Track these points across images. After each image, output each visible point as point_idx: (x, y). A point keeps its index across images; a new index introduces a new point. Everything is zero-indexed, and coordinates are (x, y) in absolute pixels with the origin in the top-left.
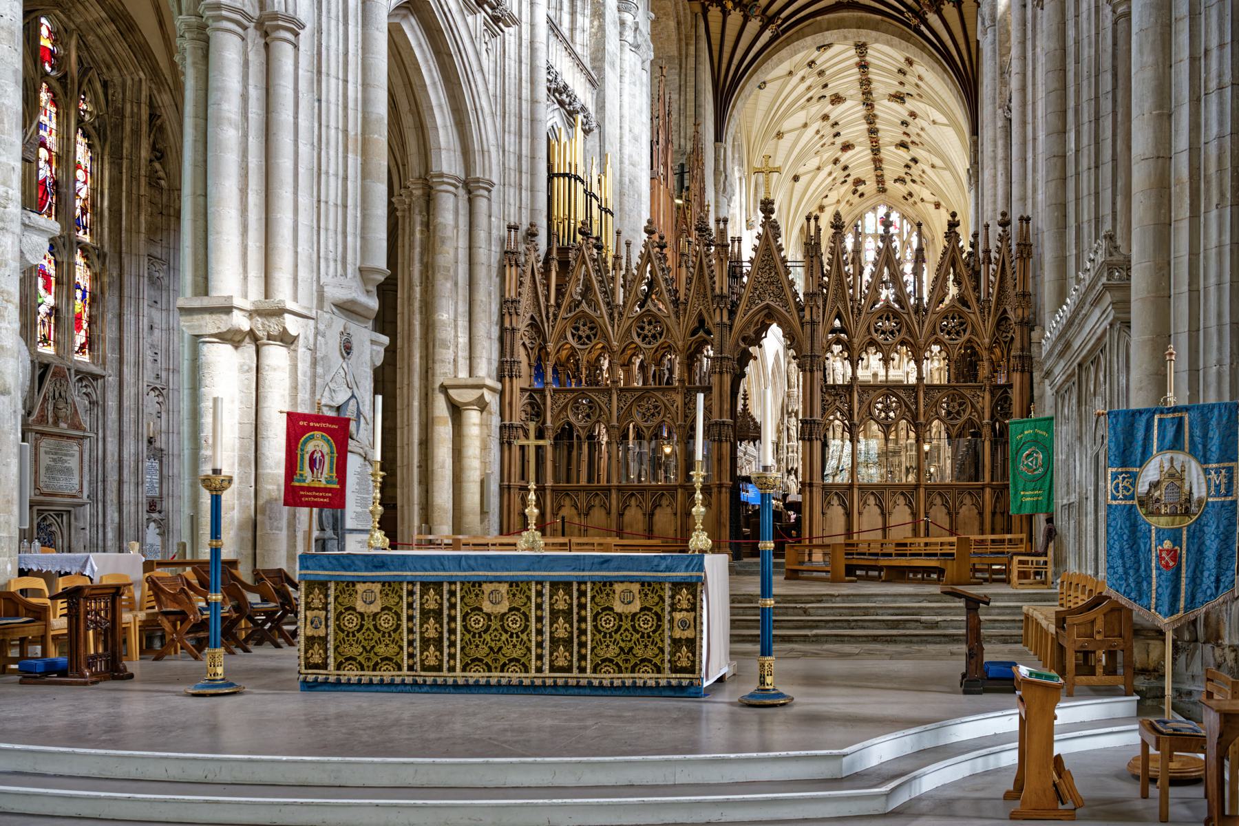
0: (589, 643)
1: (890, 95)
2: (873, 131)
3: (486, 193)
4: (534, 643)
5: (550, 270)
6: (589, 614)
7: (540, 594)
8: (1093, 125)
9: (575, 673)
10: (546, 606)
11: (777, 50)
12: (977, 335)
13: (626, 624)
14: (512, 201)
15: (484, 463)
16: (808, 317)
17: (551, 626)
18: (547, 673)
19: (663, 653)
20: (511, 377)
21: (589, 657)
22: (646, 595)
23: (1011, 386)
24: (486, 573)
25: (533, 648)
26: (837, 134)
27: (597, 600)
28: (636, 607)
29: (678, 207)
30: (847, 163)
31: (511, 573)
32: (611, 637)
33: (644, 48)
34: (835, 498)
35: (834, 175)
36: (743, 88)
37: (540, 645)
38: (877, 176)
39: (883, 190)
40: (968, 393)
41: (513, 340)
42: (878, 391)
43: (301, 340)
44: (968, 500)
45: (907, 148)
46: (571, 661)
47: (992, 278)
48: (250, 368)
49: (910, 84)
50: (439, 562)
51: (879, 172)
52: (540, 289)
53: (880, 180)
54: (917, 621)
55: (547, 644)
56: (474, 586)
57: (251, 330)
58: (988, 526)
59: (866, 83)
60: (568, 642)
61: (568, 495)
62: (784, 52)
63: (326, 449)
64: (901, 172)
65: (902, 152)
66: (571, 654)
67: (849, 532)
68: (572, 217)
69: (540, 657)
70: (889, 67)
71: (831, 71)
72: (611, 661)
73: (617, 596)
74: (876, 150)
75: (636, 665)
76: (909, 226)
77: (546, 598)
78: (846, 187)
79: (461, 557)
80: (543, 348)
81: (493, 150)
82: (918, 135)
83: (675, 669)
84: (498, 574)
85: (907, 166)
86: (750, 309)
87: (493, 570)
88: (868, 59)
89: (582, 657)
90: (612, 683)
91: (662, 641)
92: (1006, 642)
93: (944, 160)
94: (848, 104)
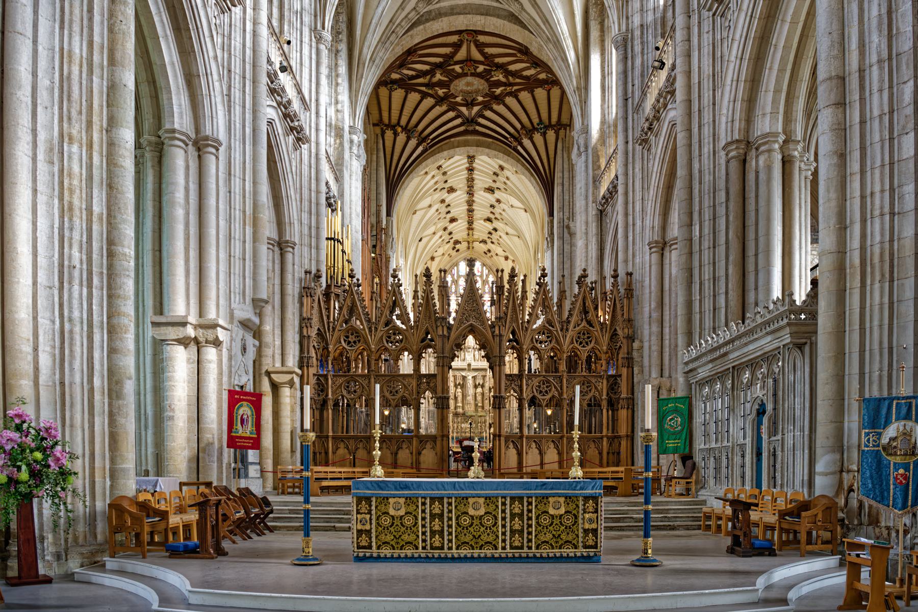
1: (486, 188)
2: (470, 211)
3: (291, 250)
4: (500, 533)
5: (330, 299)
6: (534, 515)
7: (504, 504)
8: (712, 222)
9: (526, 550)
10: (508, 511)
11: (425, 159)
12: (598, 344)
13: (557, 521)
15: (293, 421)
16: (497, 332)
17: (511, 522)
18: (508, 550)
19: (578, 537)
20: (308, 367)
21: (533, 540)
22: (568, 504)
24: (471, 492)
25: (500, 536)
26: (449, 212)
27: (539, 507)
28: (562, 511)
29: (374, 258)
31: (487, 492)
32: (547, 528)
33: (362, 157)
35: (443, 238)
36: (404, 182)
37: (504, 534)
40: (593, 380)
41: (309, 343)
42: (538, 378)
43: (224, 344)
44: (592, 445)
46: (523, 543)
47: (607, 309)
48: (194, 361)
49: (500, 182)
50: (526, 486)
52: (324, 311)
54: (631, 518)
55: (508, 533)
56: (463, 499)
57: (195, 337)
58: (605, 461)
59: (470, 181)
61: (342, 441)
62: (429, 161)
63: (249, 413)
64: (485, 236)
65: (488, 224)
66: (523, 539)
69: (504, 541)
71: (451, 172)
72: (547, 542)
73: (551, 505)
74: (470, 223)
75: (562, 544)
77: (508, 507)
78: (449, 245)
79: (455, 482)
80: (326, 348)
81: (296, 222)
82: (500, 214)
83: (585, 547)
84: (479, 492)
85: (490, 233)
87: (475, 490)
88: (474, 165)
89: (530, 541)
90: (548, 555)
91: (578, 530)
92: (688, 529)
93: (516, 230)
94: (458, 193)
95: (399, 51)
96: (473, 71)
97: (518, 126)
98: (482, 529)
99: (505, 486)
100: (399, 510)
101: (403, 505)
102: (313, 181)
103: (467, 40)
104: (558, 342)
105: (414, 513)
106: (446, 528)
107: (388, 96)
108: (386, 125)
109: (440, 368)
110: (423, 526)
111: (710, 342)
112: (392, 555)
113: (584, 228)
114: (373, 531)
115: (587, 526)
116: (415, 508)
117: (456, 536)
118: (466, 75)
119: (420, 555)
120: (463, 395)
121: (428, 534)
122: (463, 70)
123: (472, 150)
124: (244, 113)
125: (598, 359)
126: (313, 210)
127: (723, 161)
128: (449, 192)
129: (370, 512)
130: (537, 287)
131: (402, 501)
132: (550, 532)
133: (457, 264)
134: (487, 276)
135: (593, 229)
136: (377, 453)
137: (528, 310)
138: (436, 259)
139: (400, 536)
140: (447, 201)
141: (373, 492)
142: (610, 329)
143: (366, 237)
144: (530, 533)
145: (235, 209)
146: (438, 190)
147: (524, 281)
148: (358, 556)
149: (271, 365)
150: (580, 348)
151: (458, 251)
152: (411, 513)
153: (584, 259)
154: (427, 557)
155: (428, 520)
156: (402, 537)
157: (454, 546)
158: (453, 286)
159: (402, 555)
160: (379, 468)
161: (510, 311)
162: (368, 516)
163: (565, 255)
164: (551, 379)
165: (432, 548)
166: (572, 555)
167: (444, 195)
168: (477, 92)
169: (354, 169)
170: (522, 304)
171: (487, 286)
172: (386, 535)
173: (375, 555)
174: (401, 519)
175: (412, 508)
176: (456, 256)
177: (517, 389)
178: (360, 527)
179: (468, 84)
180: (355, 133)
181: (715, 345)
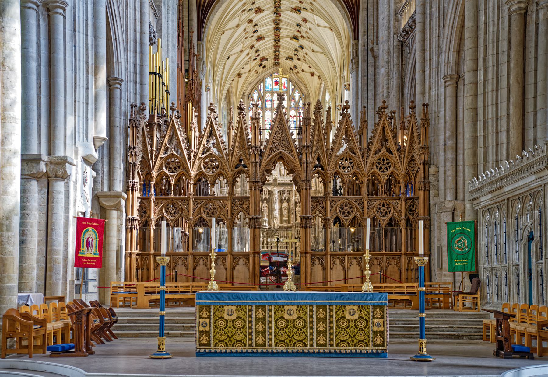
0: (334, 333)
1: (292, 8)
2: (277, 29)
4: (309, 333)
5: (153, 130)
6: (334, 320)
7: (311, 311)
9: (328, 347)
10: (314, 316)
12: (397, 169)
16: (304, 159)
17: (317, 325)
18: (315, 347)
19: (369, 337)
21: (334, 339)
22: (361, 311)
23: (417, 198)
24: (287, 301)
25: (309, 336)
26: (256, 31)
27: (338, 313)
28: (356, 316)
29: (187, 83)
30: (258, 48)
31: (299, 301)
34: (317, 260)
35: (250, 55)
37: (312, 334)
38: (275, 55)
39: (277, 64)
42: (341, 200)
45: (298, 40)
46: (326, 341)
48: (45, 192)
49: (307, 3)
50: (329, 297)
51: (277, 53)
53: (277, 58)
55: (315, 334)
60: (325, 333)
63: (94, 237)
64: (292, 54)
66: (326, 338)
67: (325, 278)
69: (312, 340)
72: (345, 341)
73: (347, 311)
76: (293, 87)
77: (314, 313)
78: (255, 61)
82: (307, 32)
84: (292, 301)
86: (271, 154)
87: (289, 300)
89: (331, 340)
90: (346, 351)
93: (322, 48)
94: (266, 13)
98: (295, 330)
99: (313, 297)
100: (231, 315)
101: (235, 312)
104: (358, 167)
105: (243, 318)
106: (267, 329)
109: (253, 191)
110: (250, 328)
111: (490, 176)
112: (226, 351)
113: (386, 57)
114: (212, 332)
115: (376, 329)
116: (244, 313)
117: (275, 336)
119: (247, 351)
120: (269, 209)
121: (254, 334)
125: (397, 182)
126: (137, 49)
127: (506, 14)
128: (256, 12)
129: (209, 317)
130: (341, 117)
131: (234, 308)
132: (347, 333)
133: (263, 80)
135: (395, 59)
136: (213, 271)
137: (332, 138)
138: (242, 76)
139: (232, 335)
140: (254, 20)
141: (212, 301)
142: (408, 155)
143: (180, 65)
144: (331, 334)
145: (79, 60)
146: (246, 11)
147: (328, 112)
148: (199, 352)
149: (100, 190)
150: (379, 172)
151: (264, 67)
152: (241, 318)
153: (385, 87)
154: (253, 352)
155: (253, 323)
156: (234, 337)
157: (273, 344)
159: (234, 351)
160: (214, 283)
161: (315, 140)
162: (208, 320)
163: (369, 77)
164: (353, 201)
165: (256, 345)
166: (364, 351)
167: (252, 15)
170: (327, 133)
171: (293, 102)
172: (221, 335)
173: (213, 351)
174: (233, 323)
175: (241, 314)
176: (262, 73)
177: (322, 210)
178: (201, 329)
181: (493, 179)
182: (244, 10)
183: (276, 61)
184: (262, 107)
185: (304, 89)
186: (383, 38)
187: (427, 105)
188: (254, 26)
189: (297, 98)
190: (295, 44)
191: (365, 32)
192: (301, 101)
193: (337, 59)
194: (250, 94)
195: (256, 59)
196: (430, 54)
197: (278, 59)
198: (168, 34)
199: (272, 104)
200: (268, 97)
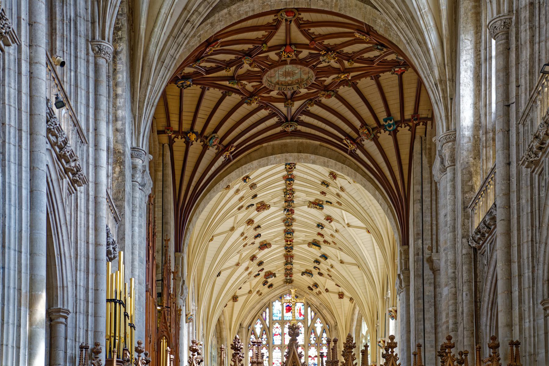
1: (310, 202)
2: (289, 232)
14: (81, 326)
26: (259, 236)
30: (262, 259)
38: (286, 269)
39: (289, 281)
45: (319, 246)
49: (332, 194)
51: (289, 266)
53: (289, 273)
64: (310, 266)
68: (117, 335)
70: (313, 179)
74: (289, 248)
76: (313, 314)
78: (258, 278)
82: (332, 235)
85: (317, 261)
93: (355, 257)
94: (272, 209)
95: (195, 43)
96: (294, 57)
97: (357, 124)
102: (91, 232)
103: (286, 20)
107: (178, 94)
108: (175, 132)
118: (284, 63)
122: (280, 57)
123: (291, 157)
124: (20, 172)
128: (258, 209)
133: (269, 305)
134: (313, 321)
135: (464, 274)
140: (256, 221)
146: (244, 208)
151: (271, 286)
158: (265, 336)
163: (426, 300)
167: (253, 213)
168: (299, 83)
169: (137, 202)
171: (313, 336)
179: (287, 74)
180: (139, 157)
182: (242, 207)
183: (288, 278)
184: (268, 343)
185: (329, 317)
186: (446, 243)
187: (517, 344)
188: (255, 229)
189: (319, 330)
190: (316, 252)
191: (418, 234)
192: (325, 335)
193: (378, 273)
194: (250, 325)
195: (259, 274)
196: (519, 267)
197: (291, 275)
198: (133, 244)
199: (283, 340)
200: (276, 329)
